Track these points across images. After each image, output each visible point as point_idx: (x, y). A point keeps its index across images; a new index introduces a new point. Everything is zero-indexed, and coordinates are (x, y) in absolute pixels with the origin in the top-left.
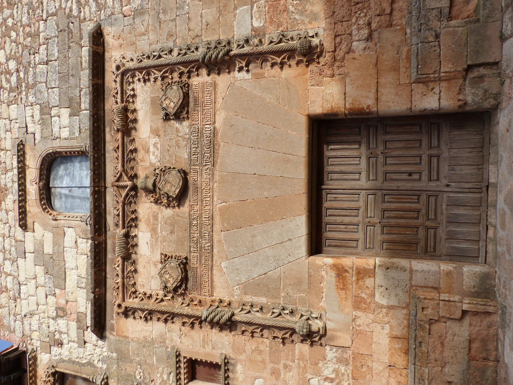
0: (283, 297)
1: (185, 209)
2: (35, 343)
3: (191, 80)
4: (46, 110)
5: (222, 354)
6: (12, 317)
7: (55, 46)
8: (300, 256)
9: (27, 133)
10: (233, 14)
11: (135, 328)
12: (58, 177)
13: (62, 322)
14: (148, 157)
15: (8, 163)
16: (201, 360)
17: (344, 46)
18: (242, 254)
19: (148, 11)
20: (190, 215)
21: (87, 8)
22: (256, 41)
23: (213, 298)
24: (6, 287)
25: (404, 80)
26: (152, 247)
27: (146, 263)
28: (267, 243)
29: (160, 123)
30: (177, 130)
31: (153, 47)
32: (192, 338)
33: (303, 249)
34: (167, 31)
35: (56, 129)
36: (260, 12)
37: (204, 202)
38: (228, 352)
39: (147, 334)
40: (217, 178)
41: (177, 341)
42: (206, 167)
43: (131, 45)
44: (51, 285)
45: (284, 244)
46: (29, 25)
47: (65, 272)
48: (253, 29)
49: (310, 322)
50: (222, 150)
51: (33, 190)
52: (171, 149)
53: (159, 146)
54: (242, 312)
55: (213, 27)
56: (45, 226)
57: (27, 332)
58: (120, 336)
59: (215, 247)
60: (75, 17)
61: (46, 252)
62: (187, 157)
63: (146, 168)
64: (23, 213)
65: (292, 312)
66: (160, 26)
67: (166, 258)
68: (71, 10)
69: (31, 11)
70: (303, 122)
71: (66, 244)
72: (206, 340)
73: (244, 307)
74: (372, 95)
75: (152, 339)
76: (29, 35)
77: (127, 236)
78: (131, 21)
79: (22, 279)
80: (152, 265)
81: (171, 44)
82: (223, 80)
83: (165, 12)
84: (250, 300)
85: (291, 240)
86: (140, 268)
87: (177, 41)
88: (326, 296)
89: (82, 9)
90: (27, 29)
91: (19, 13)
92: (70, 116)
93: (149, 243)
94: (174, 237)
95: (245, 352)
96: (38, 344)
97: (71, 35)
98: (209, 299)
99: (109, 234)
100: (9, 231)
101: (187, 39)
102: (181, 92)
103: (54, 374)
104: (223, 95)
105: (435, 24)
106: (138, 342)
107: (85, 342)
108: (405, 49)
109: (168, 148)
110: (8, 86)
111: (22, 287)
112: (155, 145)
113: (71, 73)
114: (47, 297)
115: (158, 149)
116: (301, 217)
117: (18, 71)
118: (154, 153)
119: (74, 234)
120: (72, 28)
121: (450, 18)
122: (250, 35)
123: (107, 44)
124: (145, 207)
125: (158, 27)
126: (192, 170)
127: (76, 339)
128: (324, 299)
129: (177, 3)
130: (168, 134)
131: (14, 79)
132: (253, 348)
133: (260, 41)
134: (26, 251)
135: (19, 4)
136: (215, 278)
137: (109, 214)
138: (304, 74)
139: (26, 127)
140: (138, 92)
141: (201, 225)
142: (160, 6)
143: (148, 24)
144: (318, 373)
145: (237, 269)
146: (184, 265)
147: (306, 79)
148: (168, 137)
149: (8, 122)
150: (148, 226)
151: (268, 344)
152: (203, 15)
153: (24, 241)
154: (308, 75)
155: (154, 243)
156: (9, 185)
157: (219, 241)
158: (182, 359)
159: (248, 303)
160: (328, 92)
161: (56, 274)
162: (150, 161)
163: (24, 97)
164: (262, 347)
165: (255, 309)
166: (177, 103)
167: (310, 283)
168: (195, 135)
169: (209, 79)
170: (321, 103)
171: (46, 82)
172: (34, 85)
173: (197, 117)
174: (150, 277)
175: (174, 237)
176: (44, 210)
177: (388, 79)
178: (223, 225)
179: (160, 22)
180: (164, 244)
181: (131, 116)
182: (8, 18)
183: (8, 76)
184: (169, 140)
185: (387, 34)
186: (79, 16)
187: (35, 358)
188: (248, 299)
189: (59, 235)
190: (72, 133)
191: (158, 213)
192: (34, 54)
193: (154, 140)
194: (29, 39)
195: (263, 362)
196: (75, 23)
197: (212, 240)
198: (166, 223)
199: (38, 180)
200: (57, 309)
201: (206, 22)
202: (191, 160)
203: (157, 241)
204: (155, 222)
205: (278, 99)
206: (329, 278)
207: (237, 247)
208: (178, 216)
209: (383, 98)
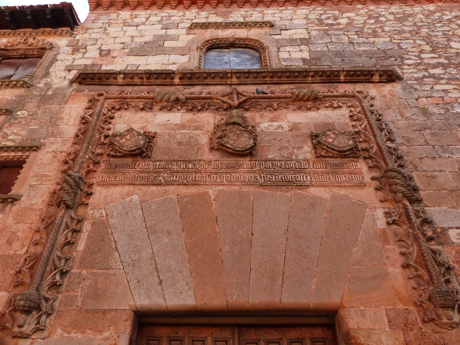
0: (80, 273)
1: (208, 155)
2: (80, 36)
3: (361, 160)
5: (21, 196)
7: (369, 48)
8: (136, 297)
9: (281, 30)
10: (456, 205)
12: (239, 54)
14: (266, 120)
16: (19, 174)
18: (147, 219)
19: (429, 119)
23: (94, 186)
26: (164, 125)
27: (147, 119)
28: (159, 251)
29: (307, 131)
30: (299, 148)
32: (49, 164)
34: (413, 136)
37: (215, 176)
39: (65, 121)
40: (245, 189)
41: (50, 148)
42: (258, 178)
43: (387, 105)
45: (155, 274)
47: (145, 55)
49: (35, 313)
52: (277, 142)
53: (279, 130)
54: (70, 219)
55: (432, 183)
57: (90, 31)
58: (69, 97)
59: (159, 188)
60: (402, 62)
62: (269, 157)
63: (253, 119)
64: (205, 26)
66: (417, 130)
69: (397, 32)
70: (331, 299)
72: (44, 178)
73: (75, 222)
75: (59, 125)
77: (177, 100)
80: (143, 125)
81: (399, 140)
82: (369, 195)
84: (84, 230)
85: (161, 283)
87: (404, 147)
88: (70, 339)
89: (412, 67)
90: (379, 30)
91: (393, 25)
93: (169, 122)
95: (17, 223)
97: (383, 58)
101: (409, 156)
102: (347, 149)
104: (351, 196)
109: (278, 139)
111: (135, 28)
114: (121, 43)
115: (276, 129)
116: (193, 298)
118: (272, 126)
120: (390, 59)
122: (435, 226)
123: (383, 86)
124: (209, 119)
125: (414, 128)
126: (254, 162)
128: (66, 335)
129: (448, 146)
130: (294, 139)
132: (18, 234)
134: (168, 30)
135: (401, 25)
136: (119, 189)
137: (202, 89)
138: (401, 300)
139: (287, 30)
140: (338, 112)
141: (186, 171)
142: (439, 130)
143: (414, 120)
145: (127, 214)
147: (395, 304)
148: (290, 138)
150: (188, 121)
151: (19, 253)
152: (443, 173)
153: (177, 28)
154: (400, 306)
155: (168, 126)
157: (165, 193)
158: (27, 154)
159: (81, 227)
160: (383, 338)
161: (143, 49)
162: (262, 123)
163: (315, 28)
164: (16, 245)
165: (70, 234)
166: (332, 145)
167: (95, 312)
168: (297, 165)
169: (367, 178)
170: (364, 327)
171: (332, 42)
172: (328, 35)
173: (320, 167)
174: (129, 122)
175: (174, 145)
176: (208, 41)
178: (186, 197)
179: (421, 130)
180: (167, 136)
181: (309, 104)
182: (386, 17)
184: (287, 139)
186: (404, 64)
188: (87, 227)
189: (182, 51)
190: (285, 60)
191: (202, 130)
192: (357, 34)
193: (286, 126)
196: (396, 62)
198: (190, 137)
199: (236, 37)
201: (437, 176)
202: (265, 161)
203: (170, 129)
204: (192, 128)
205: (358, 263)
207: (157, 213)
208: (199, 149)
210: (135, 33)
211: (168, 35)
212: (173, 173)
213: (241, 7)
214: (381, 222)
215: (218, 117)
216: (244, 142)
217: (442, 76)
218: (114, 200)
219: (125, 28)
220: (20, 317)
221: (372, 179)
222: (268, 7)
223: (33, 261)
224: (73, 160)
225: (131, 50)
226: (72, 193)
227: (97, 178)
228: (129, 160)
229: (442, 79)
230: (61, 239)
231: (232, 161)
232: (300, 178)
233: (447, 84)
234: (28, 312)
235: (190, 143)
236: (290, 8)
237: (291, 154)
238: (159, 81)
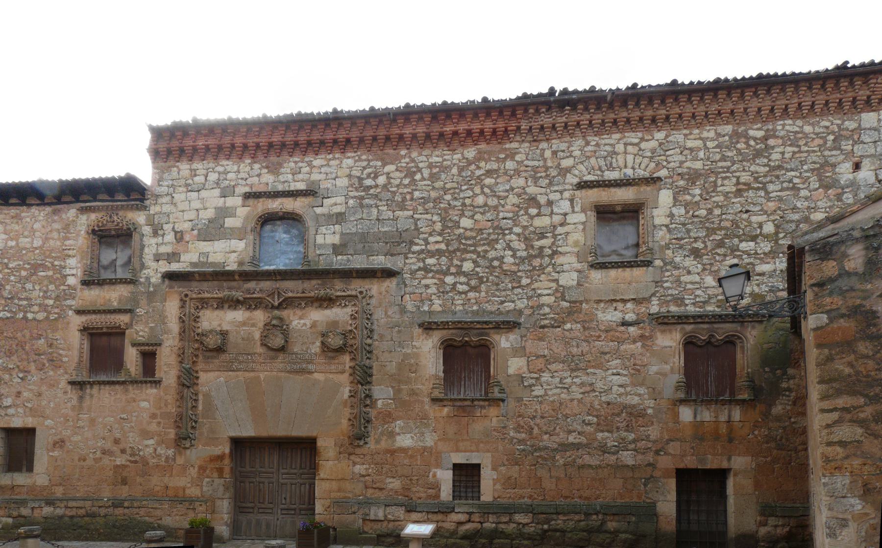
1: (260, 350)
3: (347, 354)
4: (340, 218)
6: (171, 182)
11: (172, 308)
13: (170, 237)
15: (300, 176)
17: (358, 460)
20: (255, 353)
21: (414, 260)
22: (368, 402)
24: (195, 175)
25: (333, 495)
29: (320, 328)
30: (314, 343)
31: (376, 322)
33: (233, 434)
35: (323, 229)
36: (389, 404)
38: (165, 383)
40: (280, 374)
44: (199, 226)
46: (412, 199)
48: (376, 400)
50: (299, 378)
51: (275, 205)
56: (247, 218)
60: (410, 248)
61: (226, 220)
63: (289, 317)
65: (193, 427)
67: (224, 334)
68: (417, 244)
70: (314, 434)
71: (233, 241)
74: (325, 477)
76: (404, 200)
77: (238, 302)
78: (397, 303)
79: (204, 194)
81: (375, 337)
82: (345, 378)
83: (399, 332)
86: (217, 312)
90: (408, 197)
92: (333, 244)
94: (240, 341)
96: (152, 212)
98: (197, 368)
99: (241, 283)
100: (242, 179)
103: (129, 229)
105: (361, 512)
106: (163, 311)
107: (158, 261)
108: (350, 495)
110: (364, 176)
111: (196, 194)
112: (305, 324)
113: (366, 245)
117: (377, 186)
119: (240, 249)
121: (364, 520)
124: (260, 316)
127: (160, 252)
131: (369, 182)
133: (367, 405)
144: (159, 443)
146: (220, 350)
149: (334, 176)
150: (248, 319)
156: (281, 178)
157: (237, 376)
164: (169, 406)
169: (347, 367)
175: (240, 341)
176: (260, 217)
177: (334, 485)
183: (372, 175)
185: (361, 485)
186: (410, 252)
187: (138, 209)
188: (201, 397)
194: (400, 200)
195: (160, 408)
197: (238, 370)
200: (181, 232)
206: (217, 450)
209: (323, 483)
210: (196, 204)
211: (228, 208)
212: (240, 362)
213: (291, 156)
214: (346, 395)
215: (267, 315)
216: (278, 341)
217: (433, 268)
218: (212, 380)
219: (189, 194)
220: (184, 442)
221: (350, 367)
222: (317, 154)
223: (180, 416)
224: (183, 353)
225: (199, 234)
226: (188, 381)
227: (200, 366)
228: (215, 354)
229: (432, 271)
230: (190, 405)
231: (272, 353)
232: (310, 367)
233: (433, 278)
234: (185, 439)
235: (249, 339)
236: (337, 156)
237: (308, 348)
238: (224, 278)
